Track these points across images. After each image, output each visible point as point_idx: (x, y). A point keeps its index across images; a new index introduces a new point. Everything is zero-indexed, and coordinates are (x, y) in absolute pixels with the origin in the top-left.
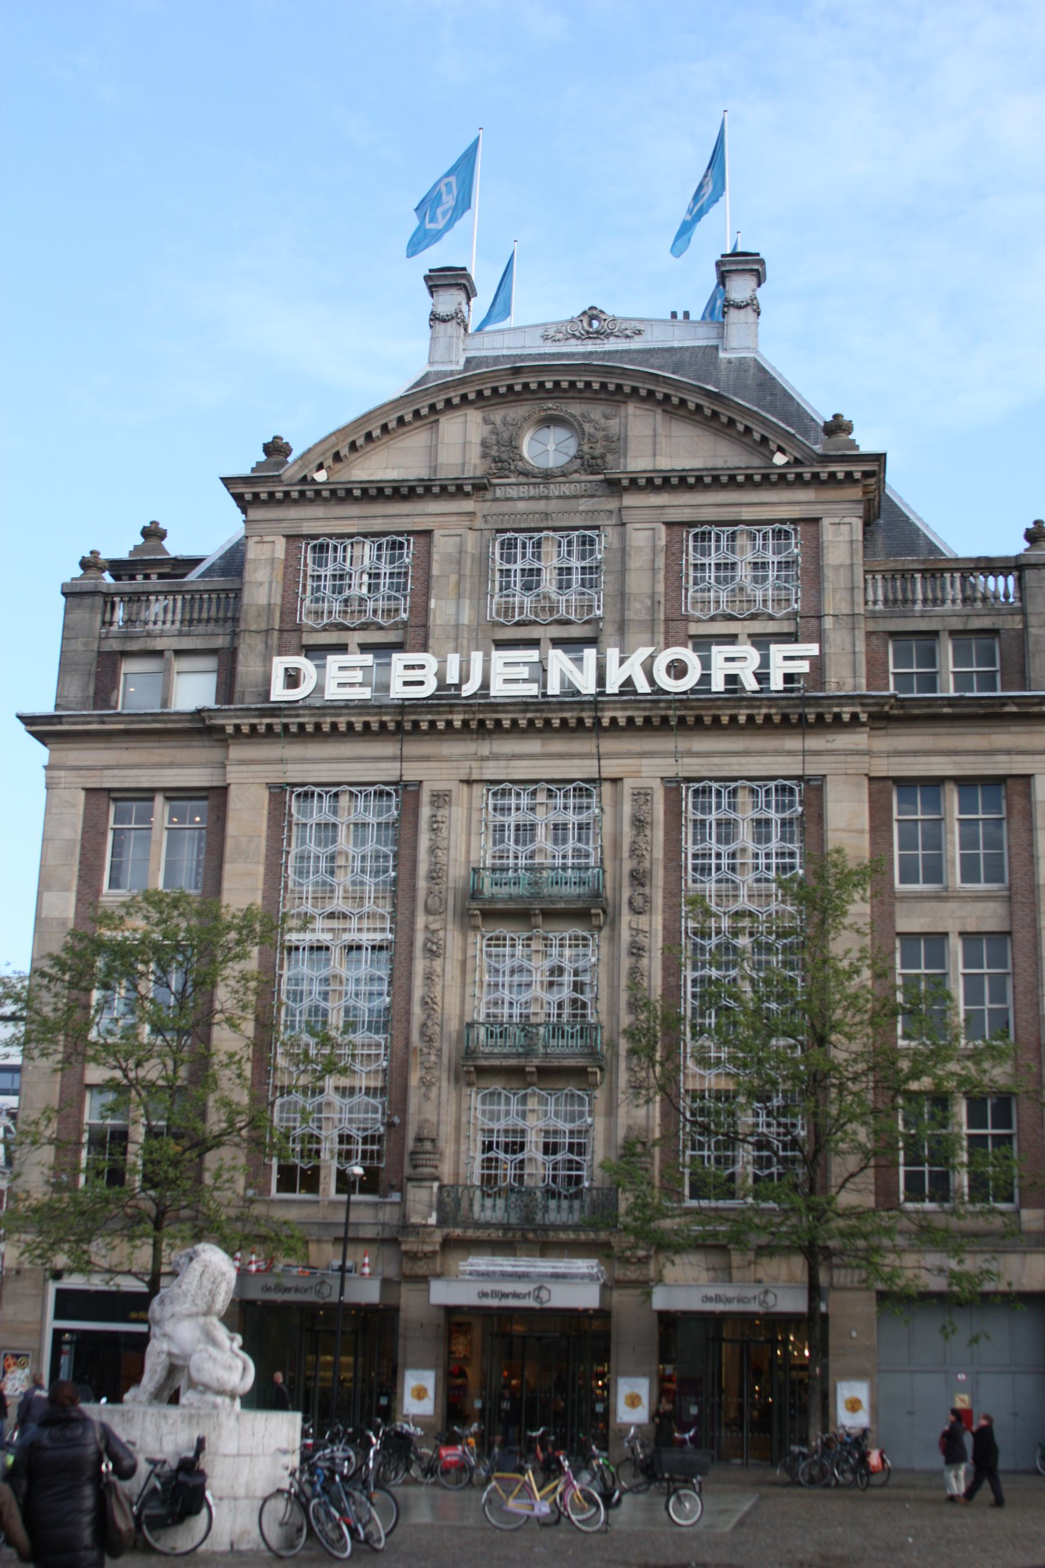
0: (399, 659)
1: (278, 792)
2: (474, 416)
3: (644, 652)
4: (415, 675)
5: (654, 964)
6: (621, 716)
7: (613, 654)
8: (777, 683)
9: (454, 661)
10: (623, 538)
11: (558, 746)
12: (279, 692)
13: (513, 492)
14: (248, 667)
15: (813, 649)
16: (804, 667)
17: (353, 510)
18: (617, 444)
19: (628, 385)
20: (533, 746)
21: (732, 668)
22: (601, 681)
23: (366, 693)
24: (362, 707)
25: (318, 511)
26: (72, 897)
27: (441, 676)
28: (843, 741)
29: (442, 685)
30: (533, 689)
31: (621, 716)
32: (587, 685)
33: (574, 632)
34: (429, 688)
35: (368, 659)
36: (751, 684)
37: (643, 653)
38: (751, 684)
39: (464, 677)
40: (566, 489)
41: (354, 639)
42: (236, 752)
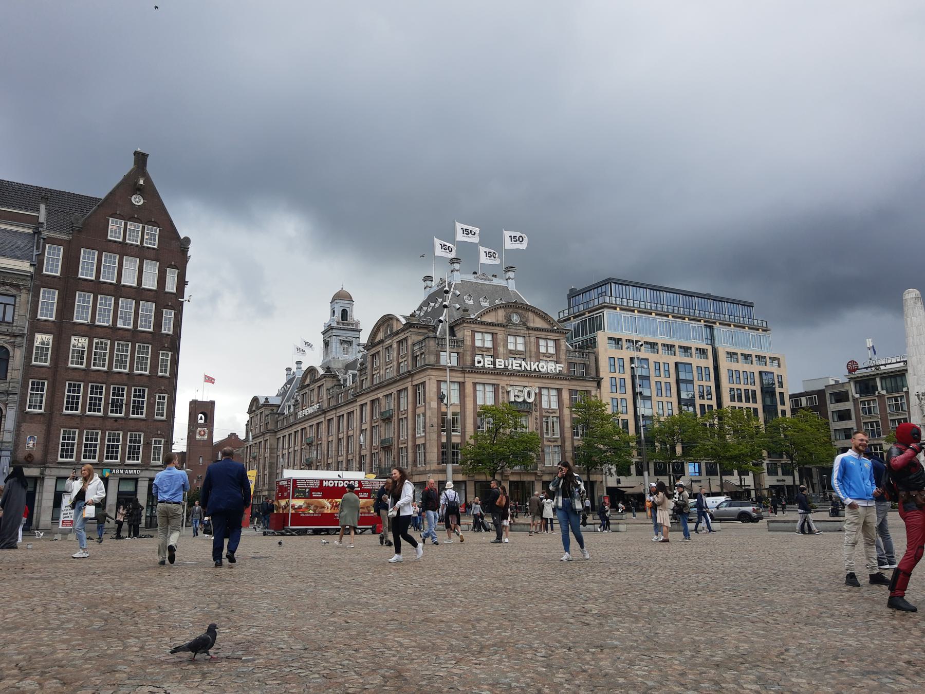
0: (497, 360)
1: (475, 384)
2: (503, 310)
3: (537, 363)
4: (500, 364)
5: (538, 421)
6: (534, 375)
7: (532, 363)
8: (558, 372)
9: (506, 361)
10: (530, 339)
11: (522, 379)
12: (477, 365)
13: (511, 327)
14: (468, 359)
15: (562, 365)
16: (561, 369)
17: (484, 327)
18: (527, 320)
19: (531, 309)
20: (517, 379)
21: (551, 368)
22: (531, 368)
23: (492, 366)
24: (492, 369)
25: (477, 326)
26: (436, 403)
27: (505, 364)
28: (565, 382)
29: (505, 366)
30: (520, 368)
31: (534, 375)
32: (529, 369)
33: (522, 356)
34: (503, 367)
35: (492, 360)
36: (554, 371)
37: (537, 363)
38: (554, 371)
39: (509, 365)
40: (520, 328)
41: (485, 353)
42: (466, 375)
